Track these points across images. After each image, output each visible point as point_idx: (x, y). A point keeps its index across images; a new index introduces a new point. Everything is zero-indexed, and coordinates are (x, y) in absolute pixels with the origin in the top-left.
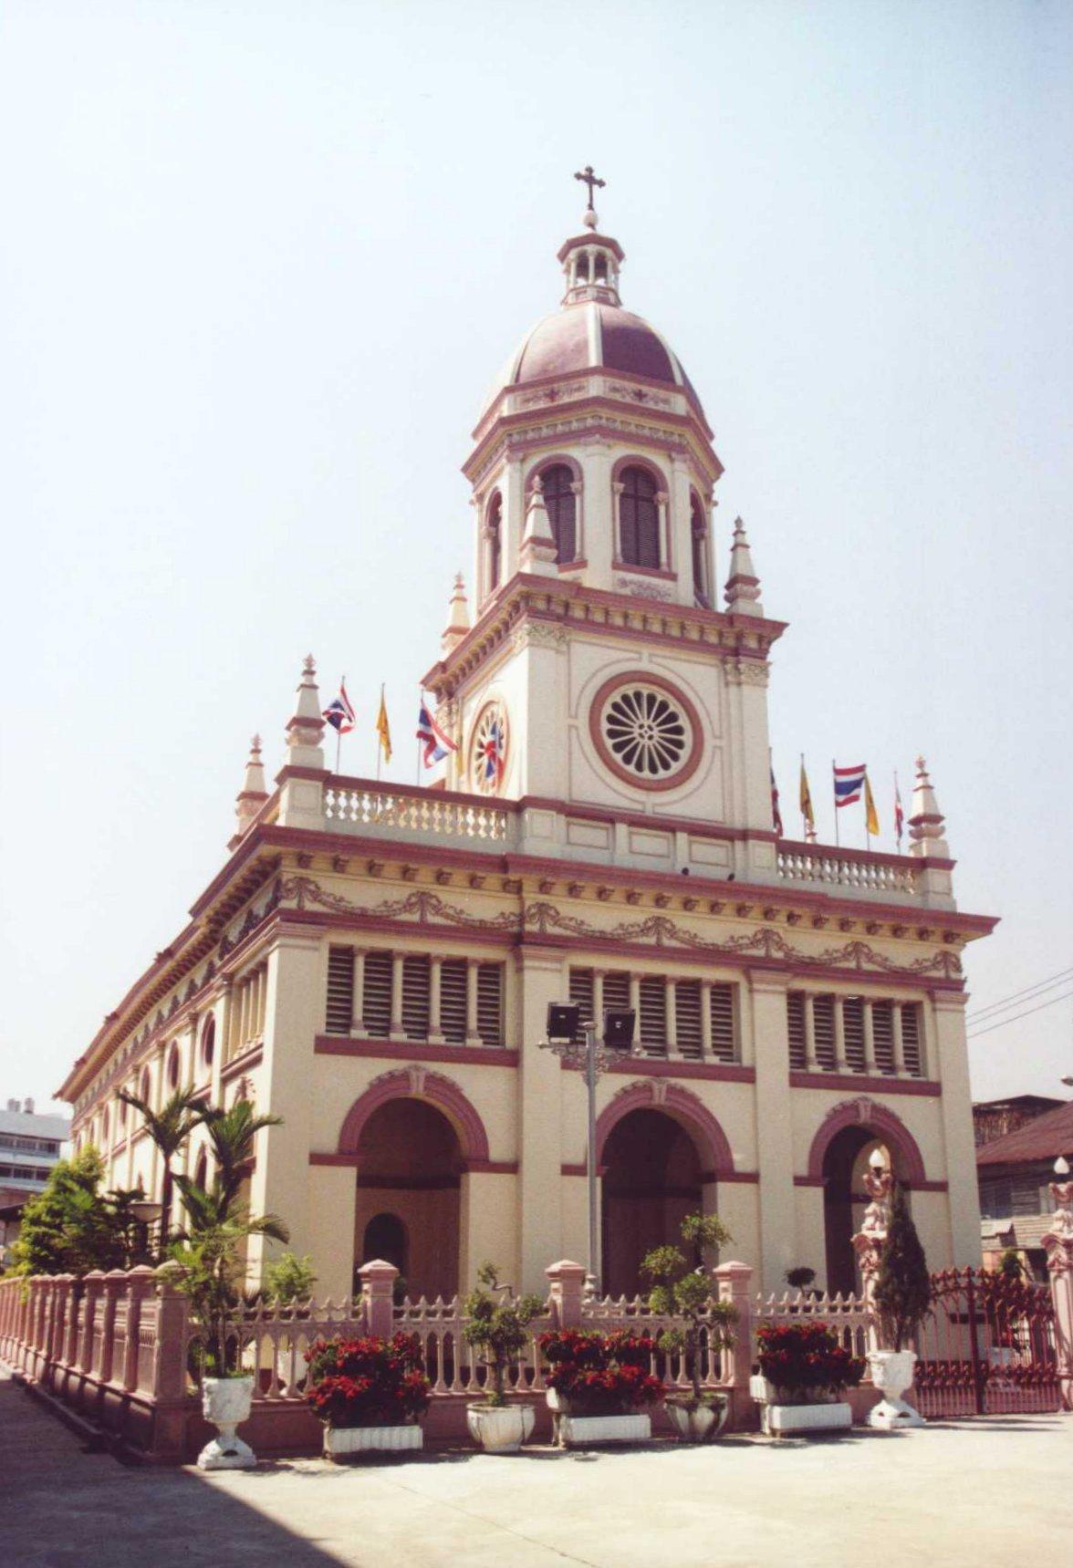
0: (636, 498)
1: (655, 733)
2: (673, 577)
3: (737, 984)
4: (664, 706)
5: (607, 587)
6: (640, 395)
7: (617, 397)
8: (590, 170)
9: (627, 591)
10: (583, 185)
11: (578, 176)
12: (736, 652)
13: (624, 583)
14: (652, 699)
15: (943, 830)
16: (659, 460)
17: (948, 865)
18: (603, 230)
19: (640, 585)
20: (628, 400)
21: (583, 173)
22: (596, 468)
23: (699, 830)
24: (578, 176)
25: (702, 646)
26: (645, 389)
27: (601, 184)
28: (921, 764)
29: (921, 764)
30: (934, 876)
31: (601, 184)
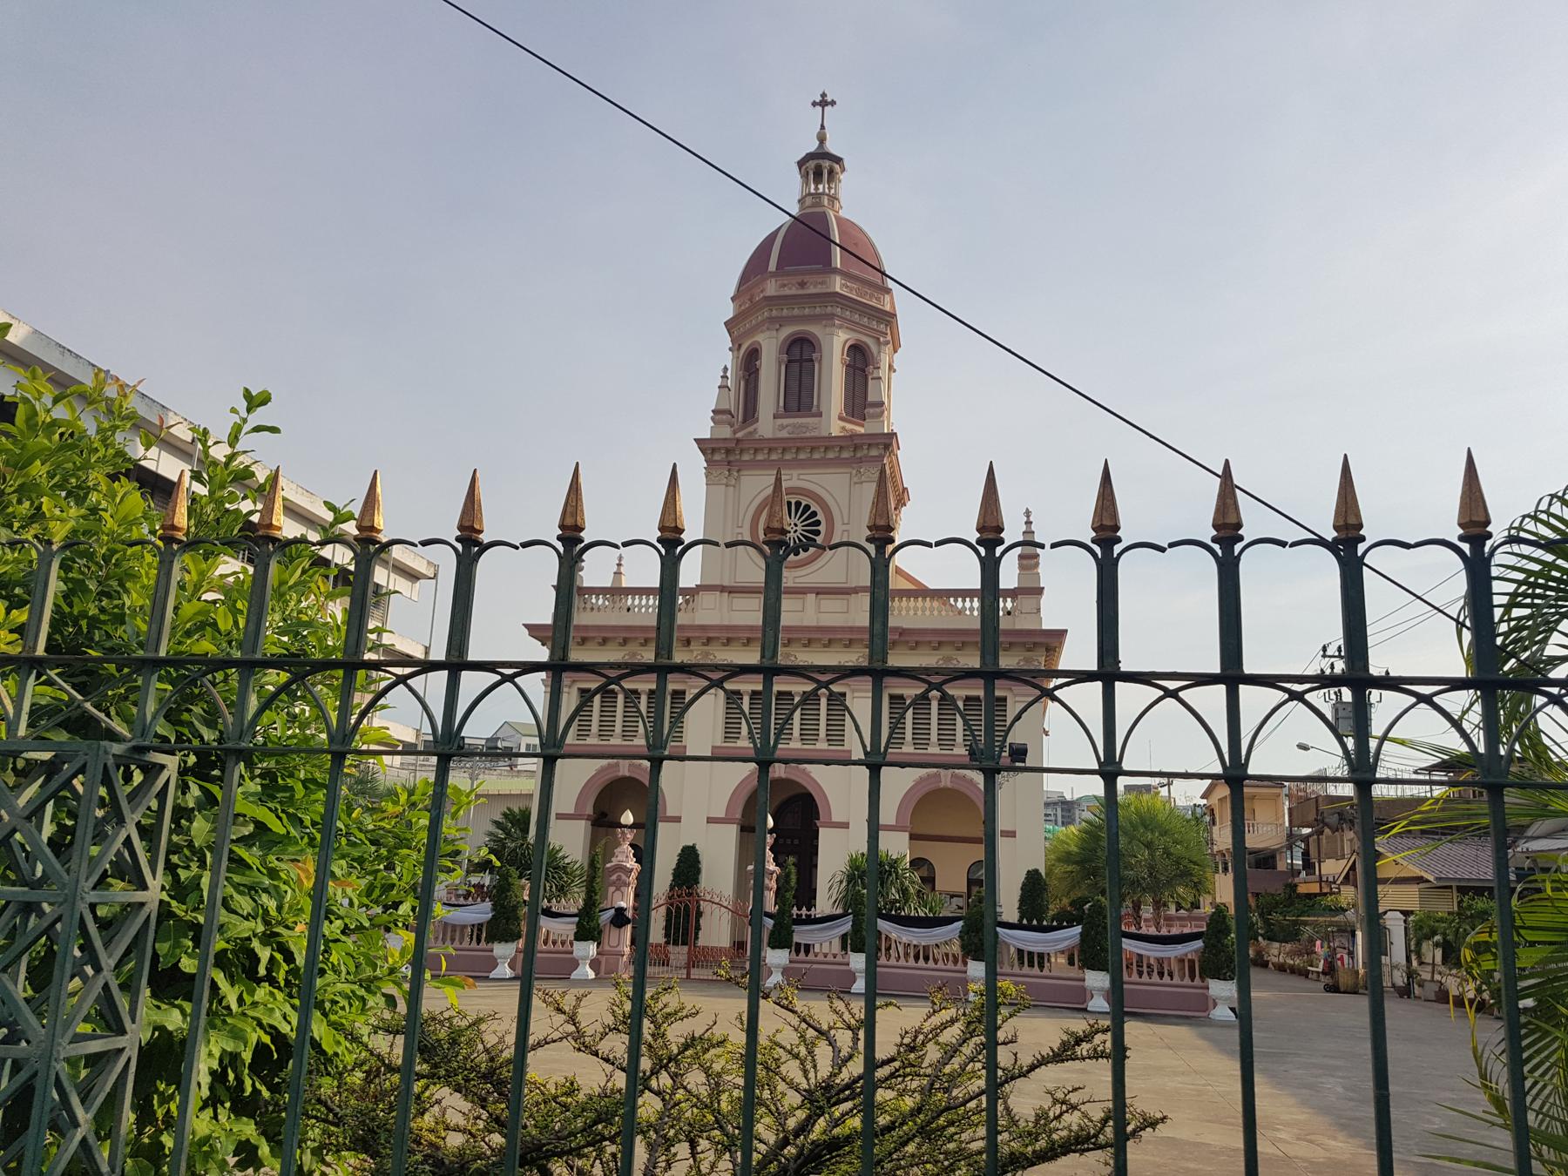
0: (801, 361)
1: (799, 528)
2: (820, 415)
3: (844, 695)
4: (807, 507)
5: (768, 435)
6: (802, 285)
7: (787, 292)
8: (824, 95)
9: (784, 434)
10: (819, 109)
11: (814, 104)
12: (860, 461)
13: (783, 427)
14: (798, 504)
15: (1037, 565)
16: (815, 330)
17: (1040, 591)
18: (832, 147)
19: (794, 425)
20: (794, 291)
21: (818, 99)
22: (770, 346)
23: (819, 592)
24: (814, 104)
25: (839, 462)
26: (806, 278)
27: (833, 103)
28: (1028, 513)
29: (1028, 513)
30: (1026, 602)
31: (833, 103)
